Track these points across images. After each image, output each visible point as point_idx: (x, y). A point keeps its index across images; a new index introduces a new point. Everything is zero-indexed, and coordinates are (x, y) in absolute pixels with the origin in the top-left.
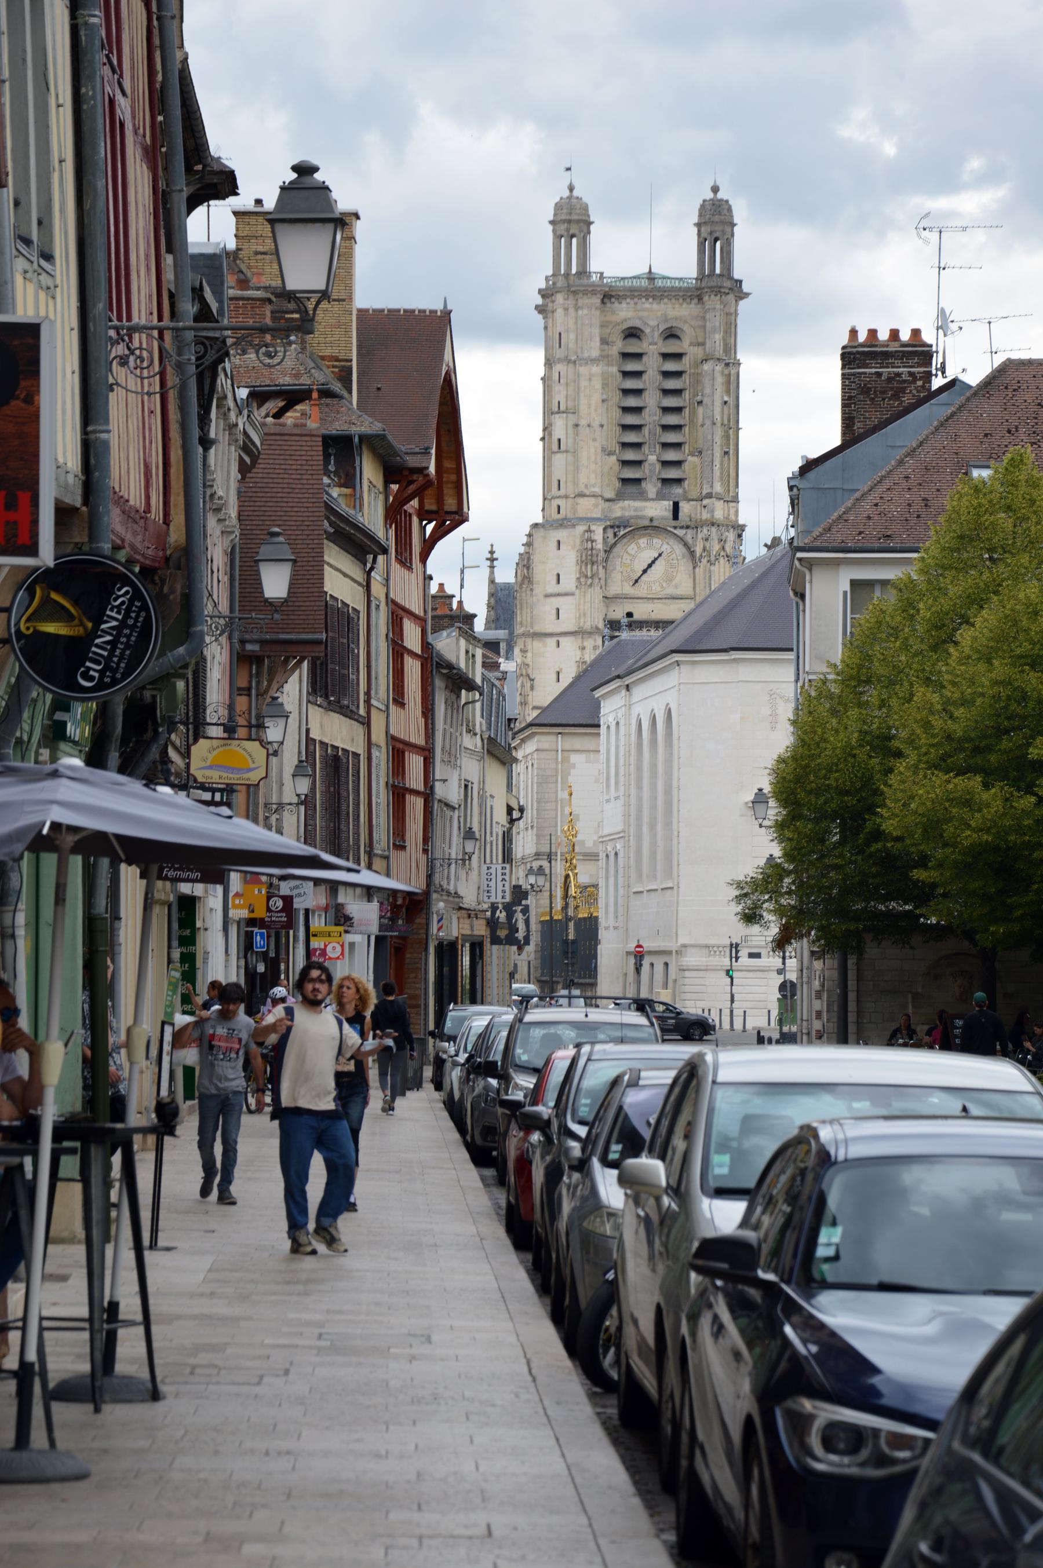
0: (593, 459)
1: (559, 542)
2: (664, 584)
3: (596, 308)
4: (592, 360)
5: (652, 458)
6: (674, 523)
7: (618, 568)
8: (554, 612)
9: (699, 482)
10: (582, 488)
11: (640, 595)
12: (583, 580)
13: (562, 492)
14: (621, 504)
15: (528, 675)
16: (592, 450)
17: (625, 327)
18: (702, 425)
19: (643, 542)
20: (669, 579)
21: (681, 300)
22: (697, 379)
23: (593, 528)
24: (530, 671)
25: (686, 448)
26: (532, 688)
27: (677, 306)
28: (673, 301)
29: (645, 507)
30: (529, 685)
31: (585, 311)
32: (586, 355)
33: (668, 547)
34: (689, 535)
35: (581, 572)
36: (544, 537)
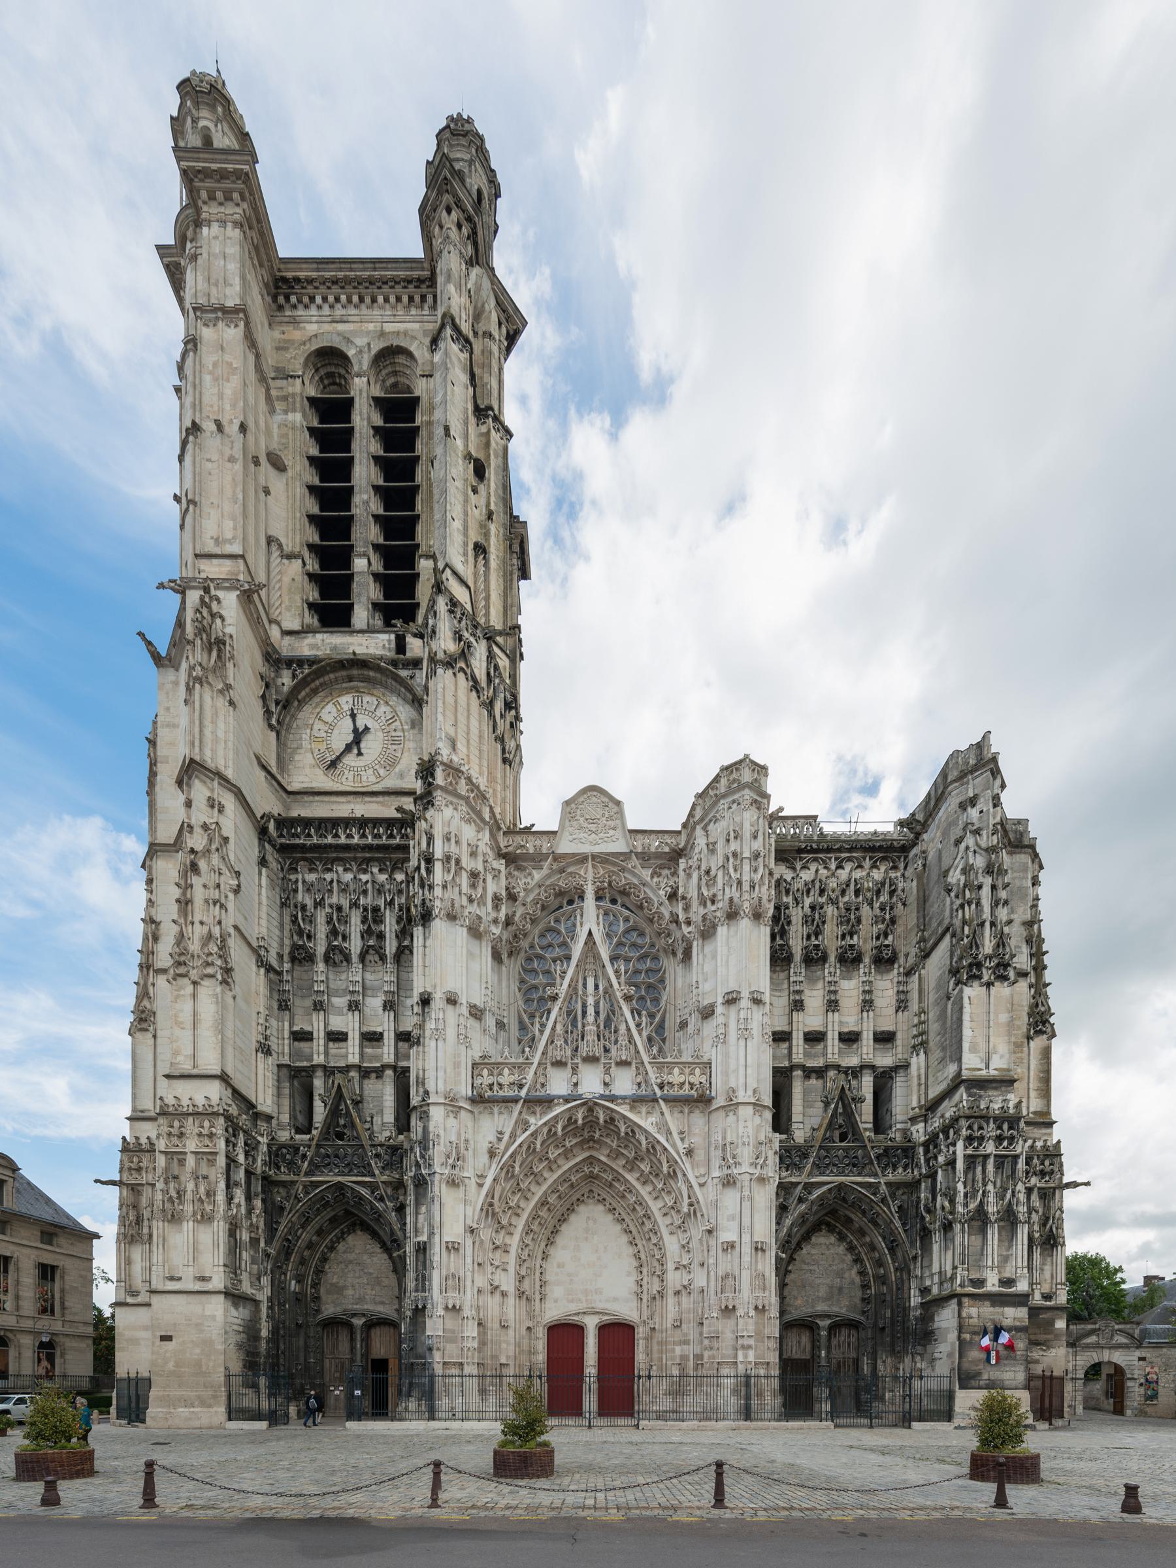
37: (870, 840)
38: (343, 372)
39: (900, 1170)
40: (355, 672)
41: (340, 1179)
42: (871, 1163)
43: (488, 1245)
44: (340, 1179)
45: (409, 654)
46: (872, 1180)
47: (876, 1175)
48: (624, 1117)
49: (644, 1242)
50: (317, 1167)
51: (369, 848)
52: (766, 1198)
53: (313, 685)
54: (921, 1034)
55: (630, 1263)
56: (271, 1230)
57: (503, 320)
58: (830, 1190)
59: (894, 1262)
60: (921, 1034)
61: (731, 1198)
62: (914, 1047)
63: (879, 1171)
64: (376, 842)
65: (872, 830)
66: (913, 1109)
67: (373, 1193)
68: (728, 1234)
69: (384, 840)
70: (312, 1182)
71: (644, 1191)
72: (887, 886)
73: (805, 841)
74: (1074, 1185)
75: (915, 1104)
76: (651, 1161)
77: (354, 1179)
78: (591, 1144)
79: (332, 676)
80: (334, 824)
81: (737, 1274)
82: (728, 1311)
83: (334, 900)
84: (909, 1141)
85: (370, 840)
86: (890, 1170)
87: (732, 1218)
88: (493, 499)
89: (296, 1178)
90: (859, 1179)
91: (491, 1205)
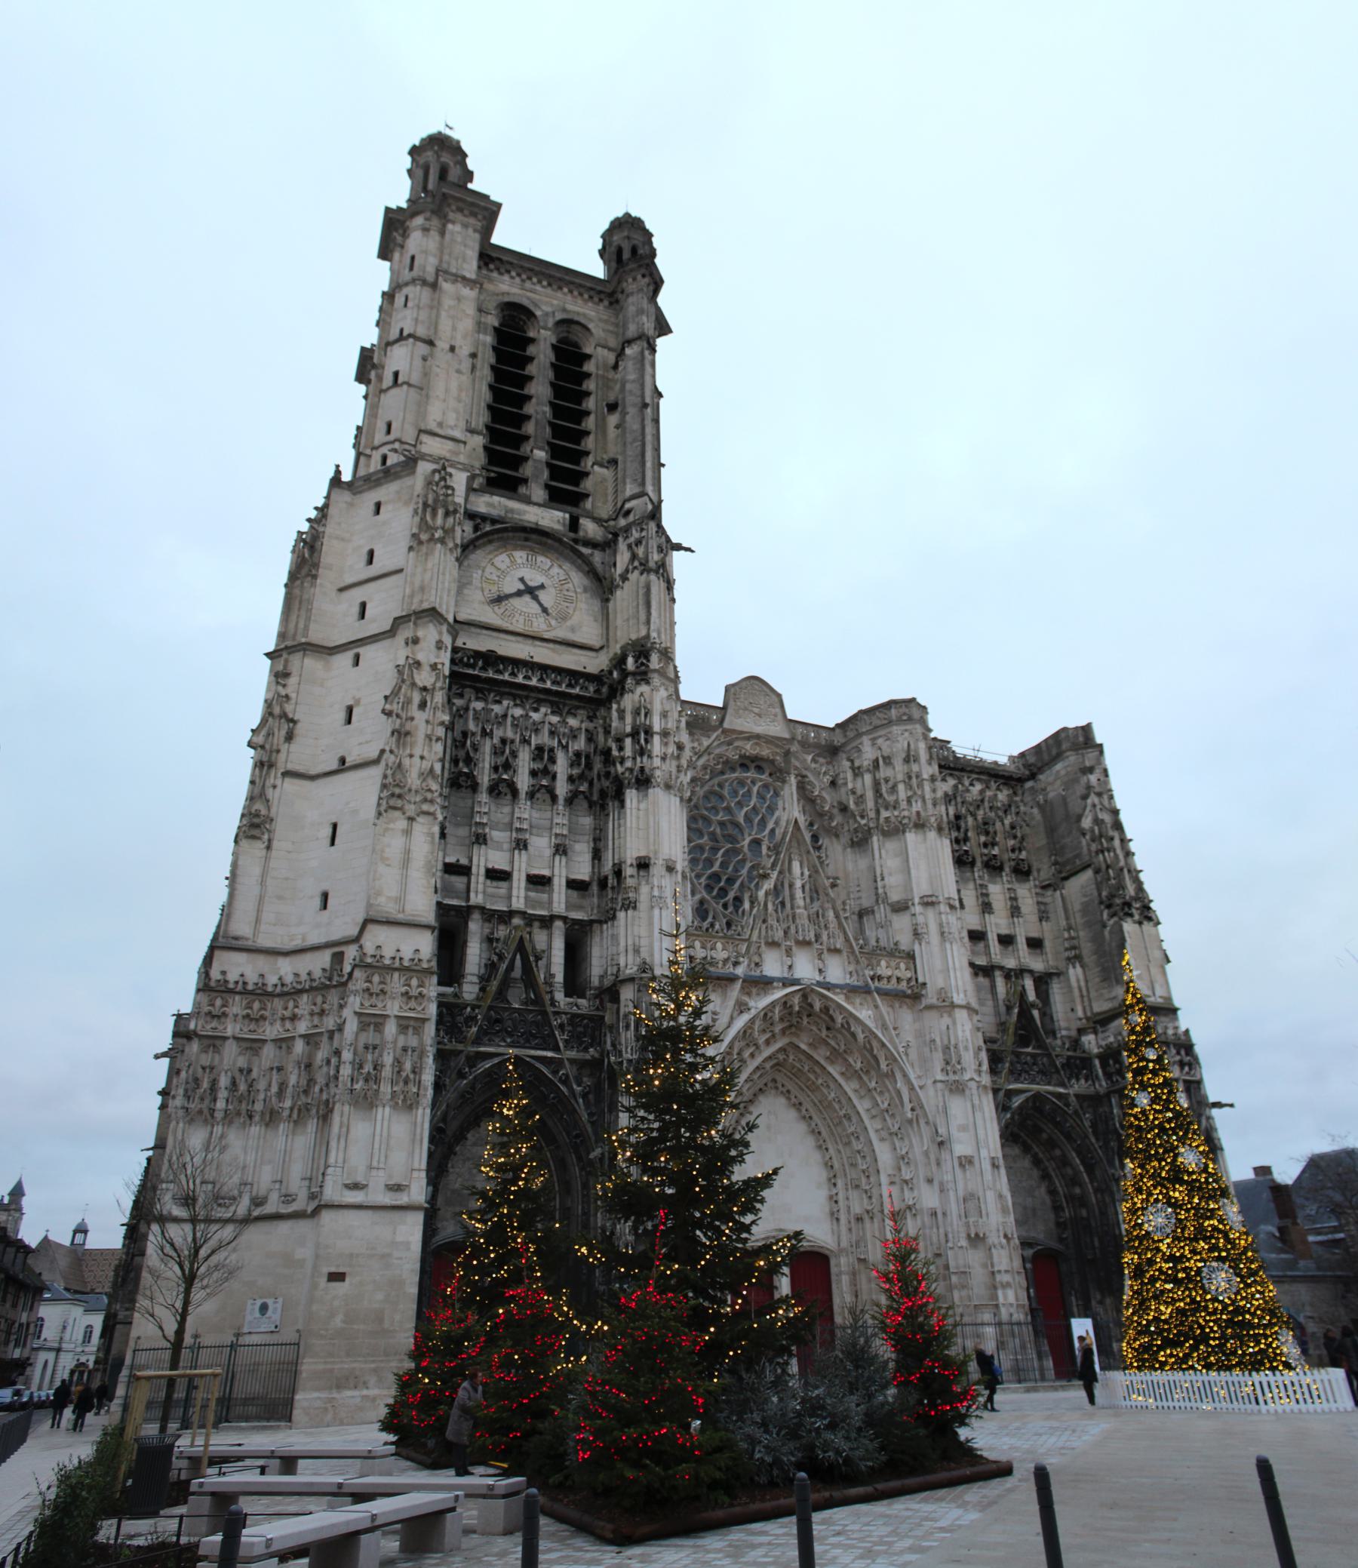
0: (454, 391)
1: (378, 506)
2: (553, 622)
3: (475, 231)
4: (464, 278)
5: (541, 455)
6: (572, 535)
7: (476, 582)
8: (356, 609)
9: (610, 498)
10: (432, 426)
11: (511, 628)
12: (424, 537)
13: (391, 437)
14: (486, 498)
15: (284, 715)
16: (454, 385)
17: (506, 299)
18: (617, 427)
19: (520, 556)
20: (563, 618)
21: (586, 296)
22: (607, 384)
24: (289, 708)
25: (590, 460)
26: (290, 737)
27: (580, 301)
28: (576, 293)
29: (525, 512)
30: (283, 733)
31: (458, 228)
32: (454, 271)
33: (561, 571)
34: (597, 557)
35: (423, 525)
36: (351, 505)
37: (993, 769)
38: (524, 318)
39: (1083, 1081)
40: (534, 536)
42: (1057, 1071)
45: (581, 533)
46: (1061, 1090)
47: (1063, 1085)
48: (839, 1006)
49: (841, 1147)
50: (486, 1033)
51: (547, 691)
52: (988, 1104)
53: (491, 538)
54: (1074, 948)
55: (821, 1175)
58: (1027, 1100)
59: (1091, 1182)
60: (1074, 948)
61: (958, 1108)
62: (1069, 959)
63: (1066, 1080)
64: (554, 688)
66: (1080, 1019)
67: (555, 1072)
68: (962, 1147)
69: (563, 688)
70: (478, 1053)
71: (849, 1087)
72: (1013, 808)
74: (1218, 1105)
75: (1080, 1013)
76: (863, 1056)
77: (533, 1052)
78: (793, 1030)
79: (511, 534)
81: (981, 1194)
82: (976, 1240)
84: (1084, 1052)
85: (548, 685)
86: (1073, 1081)
87: (963, 1128)
89: (460, 1047)
90: (1050, 1088)
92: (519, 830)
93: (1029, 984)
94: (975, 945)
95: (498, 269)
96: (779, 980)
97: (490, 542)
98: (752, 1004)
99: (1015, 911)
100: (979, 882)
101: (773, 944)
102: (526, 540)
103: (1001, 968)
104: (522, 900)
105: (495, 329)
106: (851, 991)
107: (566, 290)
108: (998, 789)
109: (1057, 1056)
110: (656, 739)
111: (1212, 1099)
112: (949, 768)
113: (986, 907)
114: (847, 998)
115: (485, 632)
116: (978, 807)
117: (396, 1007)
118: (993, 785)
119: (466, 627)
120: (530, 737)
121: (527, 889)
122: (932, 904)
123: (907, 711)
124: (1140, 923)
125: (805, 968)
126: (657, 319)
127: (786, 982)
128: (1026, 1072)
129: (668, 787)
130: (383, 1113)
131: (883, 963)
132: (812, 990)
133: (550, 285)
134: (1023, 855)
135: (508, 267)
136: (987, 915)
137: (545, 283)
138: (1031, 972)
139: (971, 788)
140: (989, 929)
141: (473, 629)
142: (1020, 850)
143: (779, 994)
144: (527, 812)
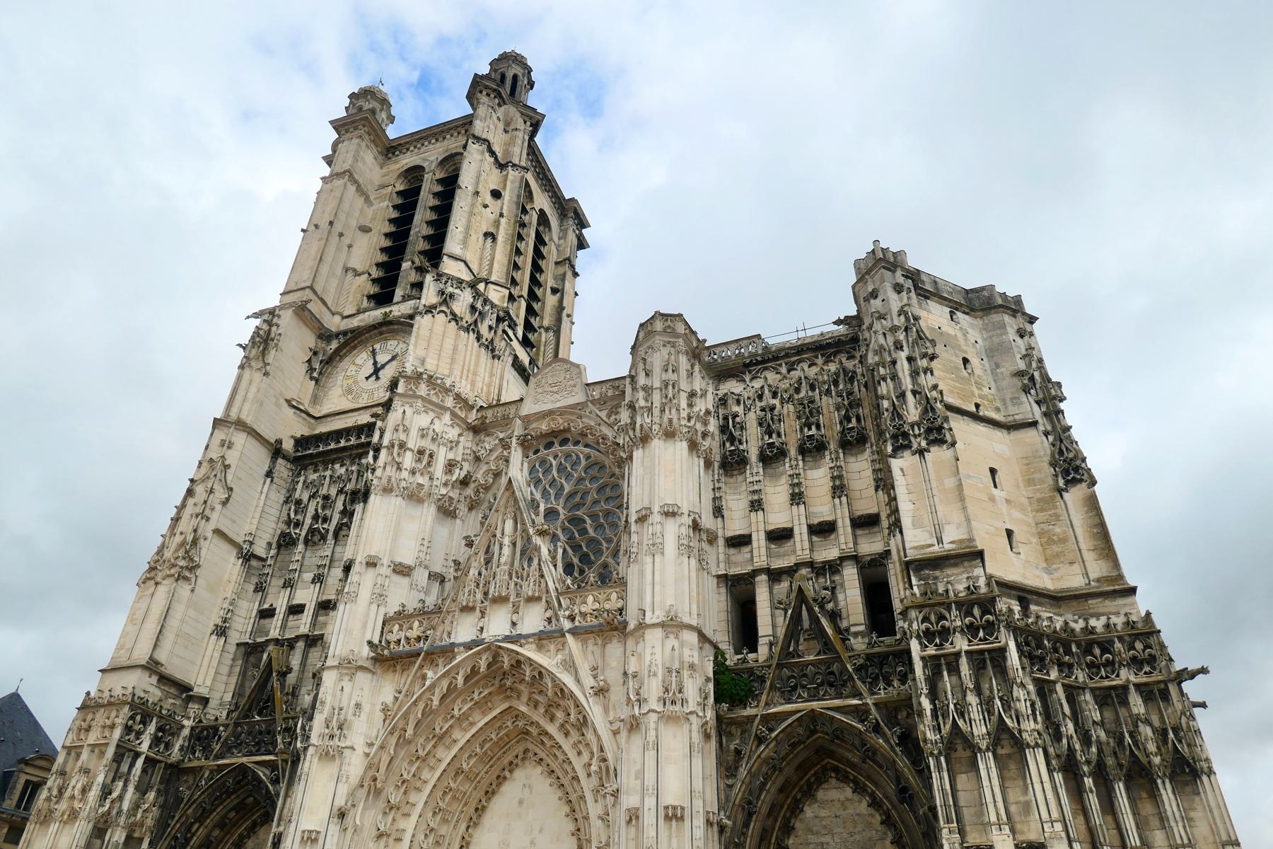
5: (406, 265)
7: (339, 383)
23: (277, 312)
39: (896, 683)
40: (384, 329)
41: (245, 760)
43: (369, 832)
44: (245, 760)
46: (855, 702)
47: (858, 695)
53: (352, 344)
56: (162, 824)
57: (526, 119)
65: (819, 333)
70: (219, 766)
73: (748, 357)
80: (338, 434)
83: (324, 491)
86: (882, 685)
88: (505, 208)
90: (837, 702)
91: (375, 780)
92: (319, 567)
93: (850, 574)
94: (780, 546)
95: (400, 152)
96: (460, 645)
97: (354, 348)
98: (430, 674)
99: (839, 489)
100: (789, 473)
101: (467, 609)
102: (381, 334)
103: (811, 564)
104: (308, 626)
105: (399, 193)
106: (541, 638)
107: (448, 136)
108: (826, 362)
109: (850, 657)
110: (383, 453)
111: (1178, 666)
112: (758, 363)
113: (797, 498)
114: (540, 648)
115: (337, 417)
116: (798, 390)
117: (94, 738)
118: (820, 361)
119: (324, 420)
120: (345, 486)
121: (316, 615)
122: (674, 514)
123: (672, 325)
124: (921, 452)
125: (497, 625)
126: (522, 114)
127: (468, 646)
128: (804, 687)
129: (387, 490)
130: (54, 827)
131: (590, 598)
132: (500, 647)
133: (437, 140)
134: (854, 422)
135: (407, 146)
136: (795, 507)
137: (433, 141)
138: (856, 558)
139: (792, 373)
140: (796, 522)
141: (329, 419)
142: (849, 421)
143: (459, 658)
144: (331, 550)
